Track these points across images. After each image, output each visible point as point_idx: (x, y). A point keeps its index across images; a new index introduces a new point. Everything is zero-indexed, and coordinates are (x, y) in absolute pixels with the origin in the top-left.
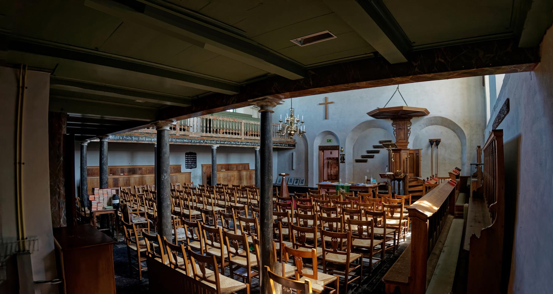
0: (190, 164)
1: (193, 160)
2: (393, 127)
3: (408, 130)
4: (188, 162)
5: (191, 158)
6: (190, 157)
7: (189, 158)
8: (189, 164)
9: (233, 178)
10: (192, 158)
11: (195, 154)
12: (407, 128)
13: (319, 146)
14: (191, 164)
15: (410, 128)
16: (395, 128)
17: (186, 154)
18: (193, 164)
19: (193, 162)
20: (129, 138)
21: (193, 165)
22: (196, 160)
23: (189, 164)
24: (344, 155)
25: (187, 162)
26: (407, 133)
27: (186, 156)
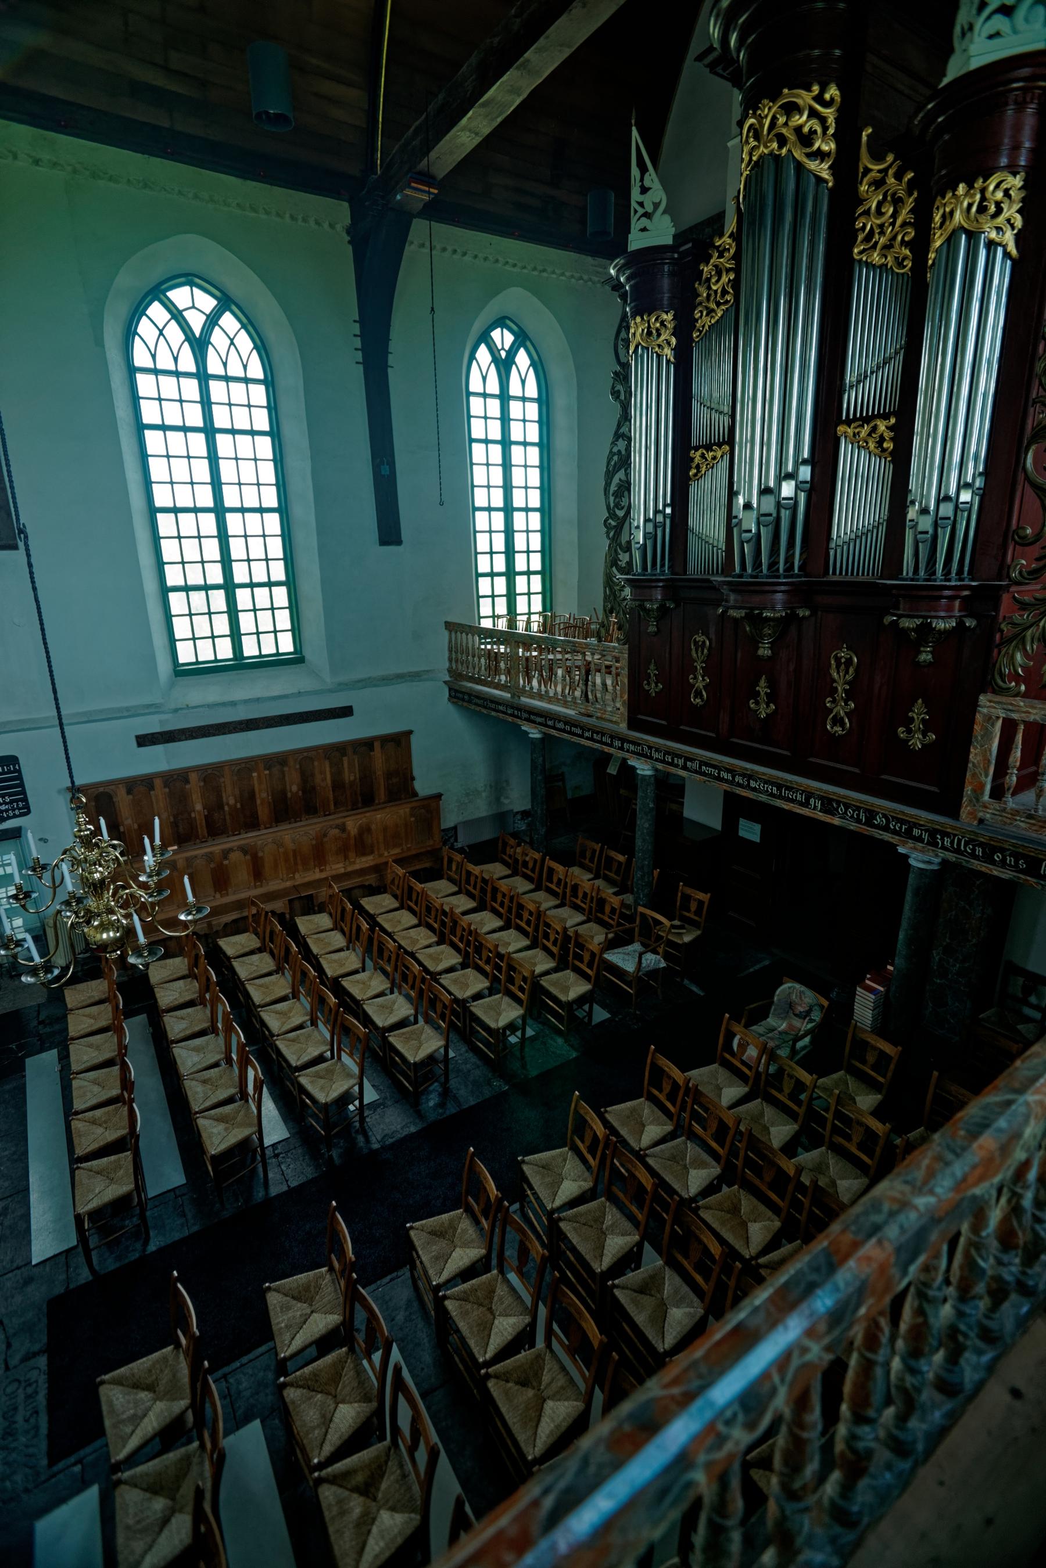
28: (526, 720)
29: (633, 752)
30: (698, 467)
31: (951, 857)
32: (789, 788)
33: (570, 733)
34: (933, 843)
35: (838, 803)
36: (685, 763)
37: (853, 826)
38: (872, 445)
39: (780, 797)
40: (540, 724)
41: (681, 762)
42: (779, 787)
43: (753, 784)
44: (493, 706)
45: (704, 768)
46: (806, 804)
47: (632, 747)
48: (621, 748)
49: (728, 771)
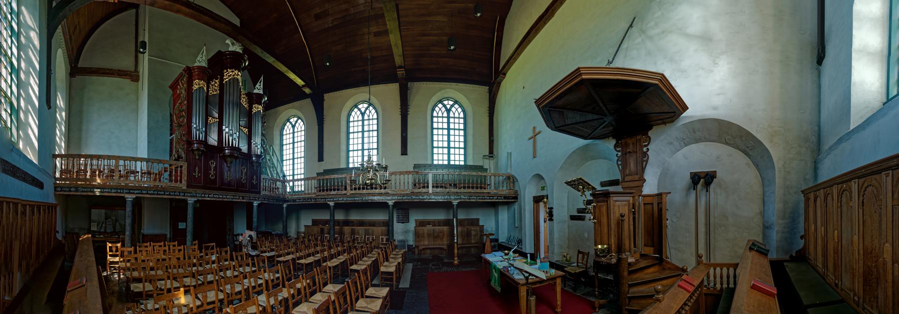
2: (616, 150)
3: (645, 154)
9: (442, 235)
12: (642, 150)
13: (534, 197)
15: (648, 149)
16: (619, 154)
20: (310, 200)
24: (552, 208)
26: (643, 160)
29: (189, 196)
32: (235, 196)
33: (158, 194)
40: (137, 193)
41: (207, 196)
46: (239, 199)
47: (189, 194)
48: (184, 196)
49: (221, 195)
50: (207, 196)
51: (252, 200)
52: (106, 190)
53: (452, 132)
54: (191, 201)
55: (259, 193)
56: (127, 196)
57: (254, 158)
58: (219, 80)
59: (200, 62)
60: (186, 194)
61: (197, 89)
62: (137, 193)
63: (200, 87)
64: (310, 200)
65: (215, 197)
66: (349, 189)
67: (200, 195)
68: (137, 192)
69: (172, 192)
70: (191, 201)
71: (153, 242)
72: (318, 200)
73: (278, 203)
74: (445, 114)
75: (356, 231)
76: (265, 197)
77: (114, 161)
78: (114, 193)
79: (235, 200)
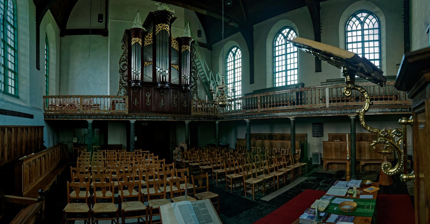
0: (316, 133)
1: (319, 130)
4: (314, 132)
5: (317, 128)
6: (316, 126)
7: (315, 128)
8: (315, 133)
10: (318, 128)
11: (322, 124)
14: (317, 133)
17: (313, 124)
18: (319, 133)
19: (319, 131)
21: (320, 134)
22: (323, 130)
23: (315, 133)
25: (313, 131)
27: (313, 126)
28: (87, 118)
30: (146, 64)
31: (192, 120)
32: (168, 117)
33: (108, 118)
34: (189, 119)
35: (176, 117)
36: (146, 118)
37: (179, 120)
38: (176, 68)
39: (167, 119)
40: (94, 118)
41: (144, 118)
42: (166, 117)
43: (161, 118)
44: (71, 117)
45: (150, 117)
48: (127, 118)
49: (156, 117)
50: (144, 118)
51: (183, 119)
52: (75, 117)
53: (366, 44)
54: (133, 121)
55: (191, 114)
56: (88, 120)
57: (183, 88)
58: (152, 33)
59: (135, 25)
60: (128, 117)
61: (134, 44)
62: (94, 118)
63: (136, 43)
64: (233, 118)
65: (151, 119)
66: (260, 107)
67: (138, 118)
68: (94, 117)
69: (118, 116)
70: (133, 121)
71: (108, 150)
72: (238, 117)
73: (209, 120)
74: (359, 27)
75: (274, 145)
76: (196, 117)
77: (80, 98)
78: (80, 118)
79: (168, 120)
